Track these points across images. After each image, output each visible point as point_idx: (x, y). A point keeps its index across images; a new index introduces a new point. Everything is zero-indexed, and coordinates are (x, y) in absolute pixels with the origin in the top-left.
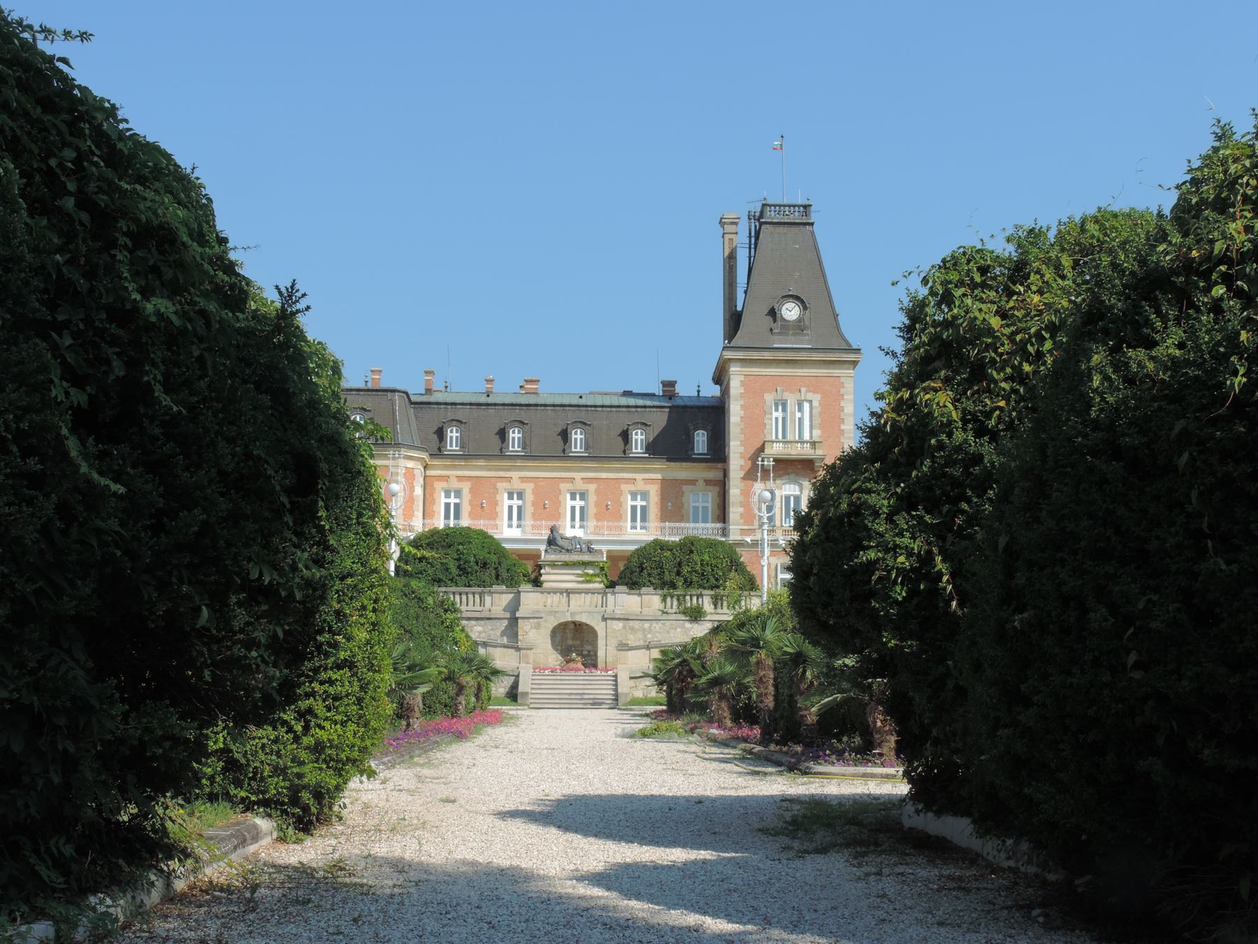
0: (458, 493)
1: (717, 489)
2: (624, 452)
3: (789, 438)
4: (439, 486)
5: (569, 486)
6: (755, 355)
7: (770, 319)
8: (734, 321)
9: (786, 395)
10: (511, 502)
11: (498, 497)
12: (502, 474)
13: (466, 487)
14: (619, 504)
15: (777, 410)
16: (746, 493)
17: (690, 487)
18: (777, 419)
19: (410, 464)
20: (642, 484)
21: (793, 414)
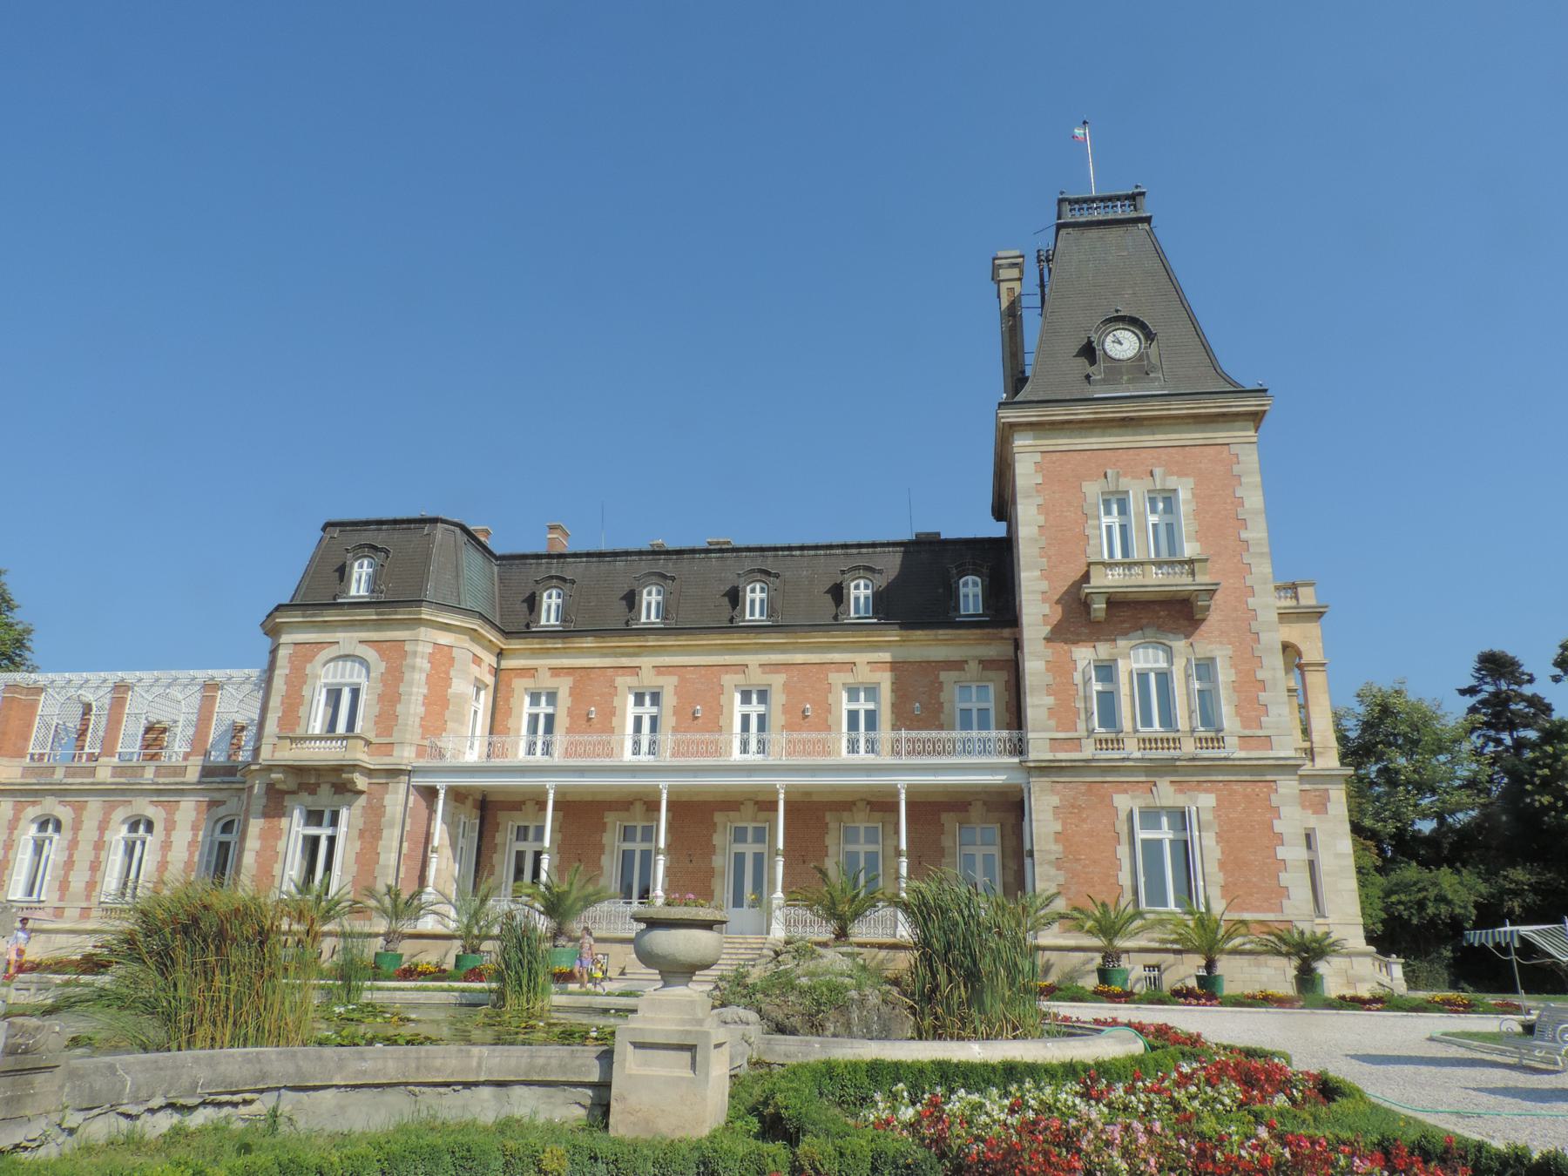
0: (552, 697)
1: (1004, 676)
2: (836, 618)
3: (1136, 555)
4: (520, 684)
5: (739, 679)
6: (1059, 414)
7: (1083, 361)
8: (1017, 380)
9: (1125, 483)
10: (639, 710)
11: (616, 702)
12: (625, 661)
13: (564, 686)
14: (827, 709)
15: (1108, 512)
16: (1061, 669)
17: (954, 675)
18: (1109, 528)
19: (445, 638)
20: (862, 670)
21: (1142, 517)
